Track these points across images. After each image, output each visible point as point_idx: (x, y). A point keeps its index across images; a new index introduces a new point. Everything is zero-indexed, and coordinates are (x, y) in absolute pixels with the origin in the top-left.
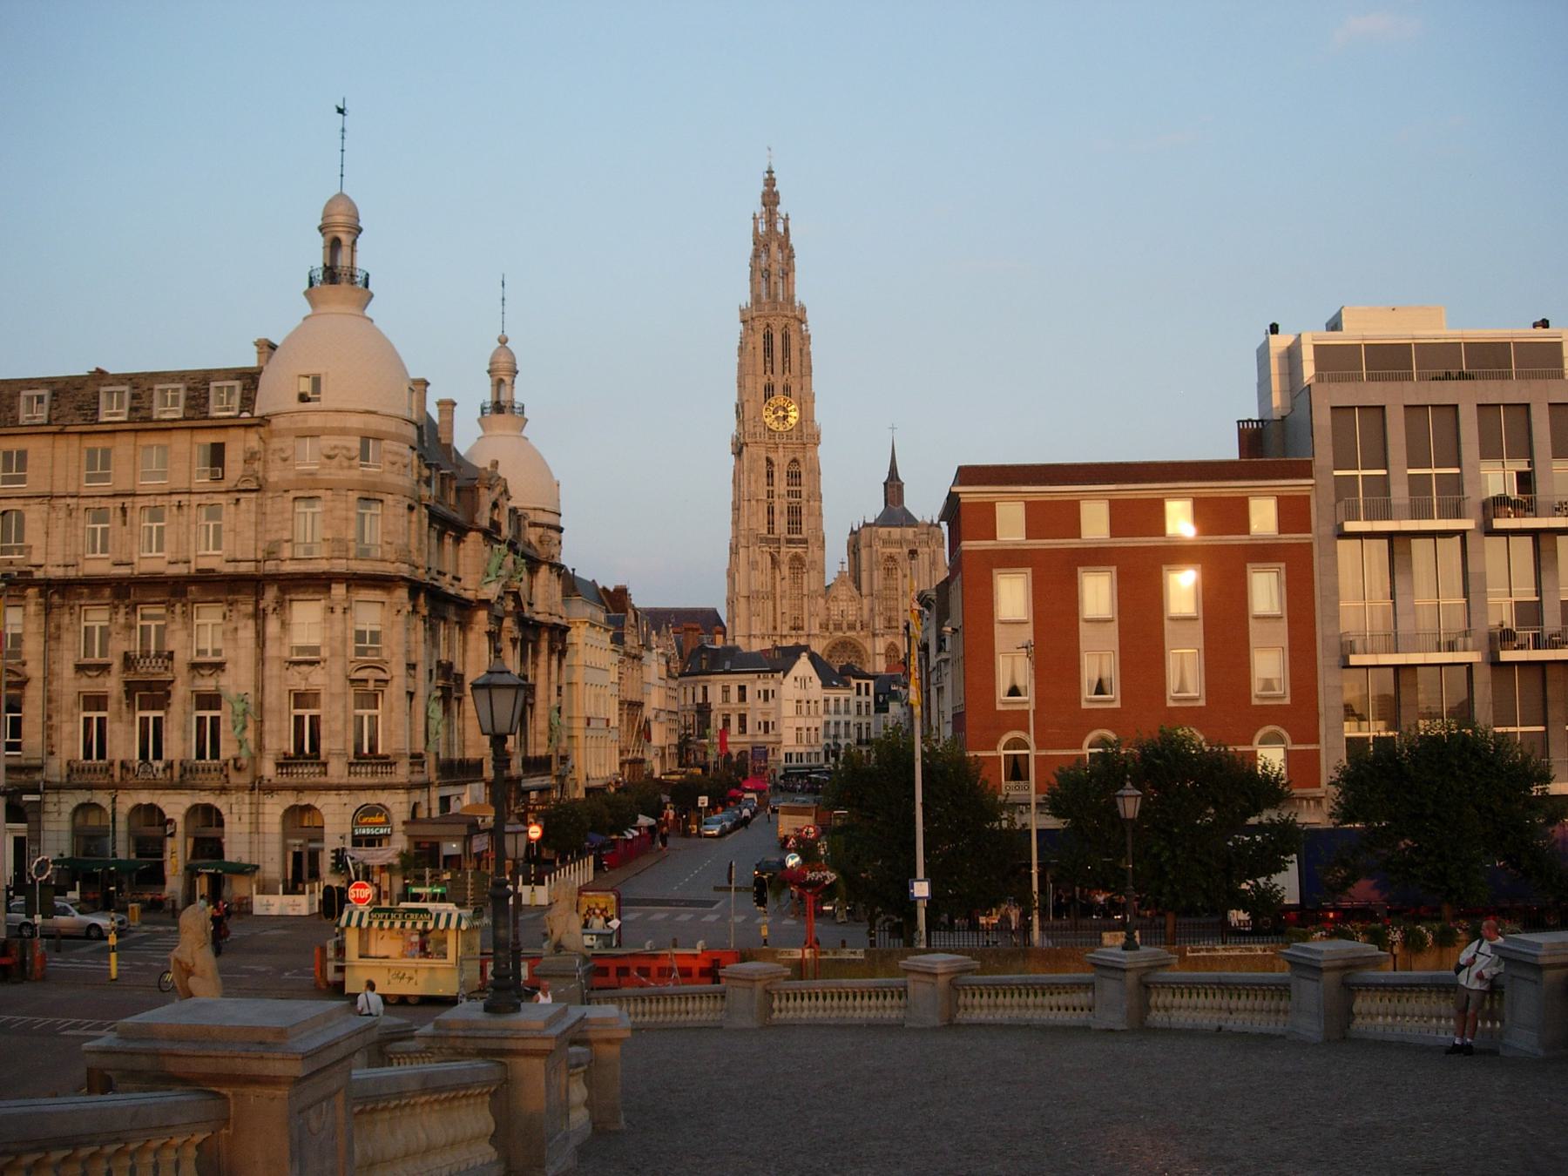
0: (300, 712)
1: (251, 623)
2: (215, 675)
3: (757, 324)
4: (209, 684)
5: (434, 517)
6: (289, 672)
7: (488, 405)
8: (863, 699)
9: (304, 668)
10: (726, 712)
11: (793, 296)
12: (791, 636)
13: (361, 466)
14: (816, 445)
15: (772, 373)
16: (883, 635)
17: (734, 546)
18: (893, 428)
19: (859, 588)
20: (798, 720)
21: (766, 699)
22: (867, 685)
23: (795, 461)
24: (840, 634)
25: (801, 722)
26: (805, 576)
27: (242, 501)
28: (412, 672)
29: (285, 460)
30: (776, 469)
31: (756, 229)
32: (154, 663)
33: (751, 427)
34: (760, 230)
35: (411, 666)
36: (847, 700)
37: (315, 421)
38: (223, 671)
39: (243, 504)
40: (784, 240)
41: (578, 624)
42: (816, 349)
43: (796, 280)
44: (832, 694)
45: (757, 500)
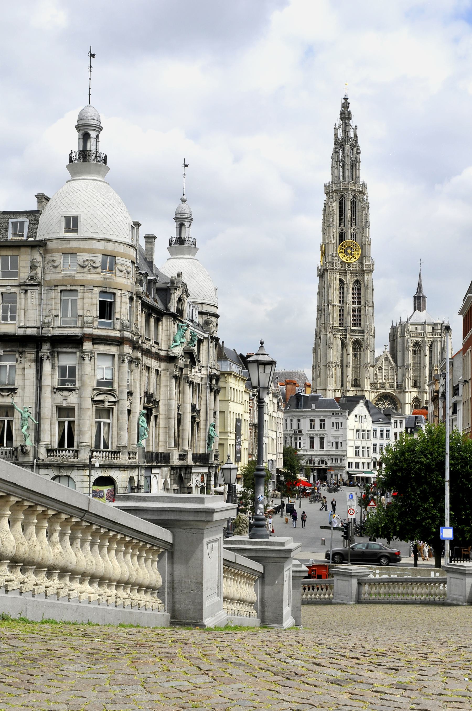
0: (62, 419)
1: (33, 365)
2: (11, 395)
3: (335, 195)
4: (7, 401)
5: (145, 305)
6: (56, 395)
7: (174, 239)
9: (65, 393)
10: (312, 436)
11: (359, 178)
13: (102, 272)
14: (371, 271)
15: (344, 226)
16: (410, 392)
17: (318, 334)
19: (396, 362)
20: (356, 442)
22: (401, 422)
23: (357, 281)
24: (384, 391)
25: (358, 443)
26: (362, 353)
27: (29, 291)
28: (130, 397)
29: (55, 267)
30: (345, 286)
31: (336, 135)
33: (330, 260)
34: (339, 136)
35: (130, 394)
36: (388, 431)
37: (74, 245)
38: (16, 393)
39: (29, 293)
41: (226, 375)
42: (371, 211)
43: (361, 168)
45: (333, 305)
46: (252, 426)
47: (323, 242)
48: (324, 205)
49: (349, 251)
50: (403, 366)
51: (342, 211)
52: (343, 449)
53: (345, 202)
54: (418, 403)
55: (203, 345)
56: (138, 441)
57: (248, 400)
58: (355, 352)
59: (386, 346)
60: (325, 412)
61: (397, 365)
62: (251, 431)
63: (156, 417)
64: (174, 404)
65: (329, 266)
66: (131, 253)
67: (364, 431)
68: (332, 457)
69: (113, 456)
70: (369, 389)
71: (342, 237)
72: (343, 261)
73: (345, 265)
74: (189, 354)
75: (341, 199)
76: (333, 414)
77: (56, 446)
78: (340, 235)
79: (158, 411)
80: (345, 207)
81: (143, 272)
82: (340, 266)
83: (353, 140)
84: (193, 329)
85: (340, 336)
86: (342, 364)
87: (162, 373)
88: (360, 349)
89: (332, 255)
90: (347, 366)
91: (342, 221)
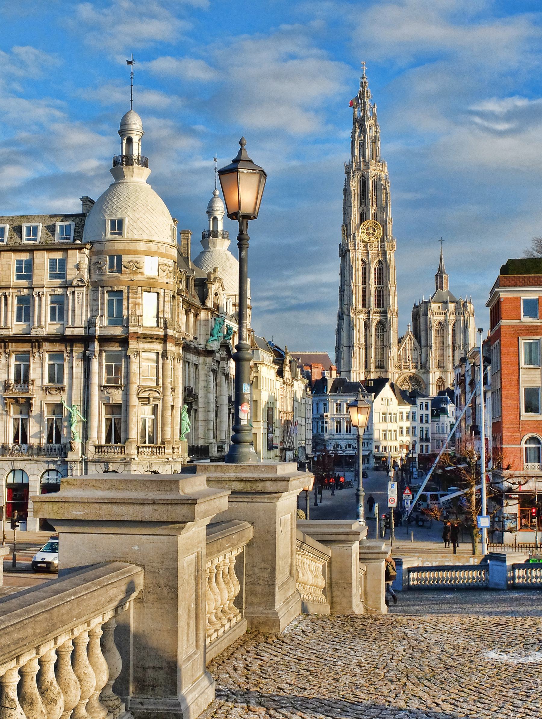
8: (424, 412)
12: (376, 372)
15: (365, 206)
19: (419, 342)
26: (385, 334)
28: (173, 393)
32: (23, 387)
35: (173, 390)
40: (373, 121)
47: (344, 222)
49: (371, 231)
50: (427, 346)
53: (365, 181)
61: (420, 346)
63: (196, 410)
64: (212, 397)
66: (173, 254)
69: (158, 451)
70: (393, 369)
73: (367, 245)
77: (103, 443)
79: (197, 404)
86: (366, 345)
87: (201, 368)
88: (383, 329)
89: (354, 236)
90: (371, 347)
91: (363, 201)
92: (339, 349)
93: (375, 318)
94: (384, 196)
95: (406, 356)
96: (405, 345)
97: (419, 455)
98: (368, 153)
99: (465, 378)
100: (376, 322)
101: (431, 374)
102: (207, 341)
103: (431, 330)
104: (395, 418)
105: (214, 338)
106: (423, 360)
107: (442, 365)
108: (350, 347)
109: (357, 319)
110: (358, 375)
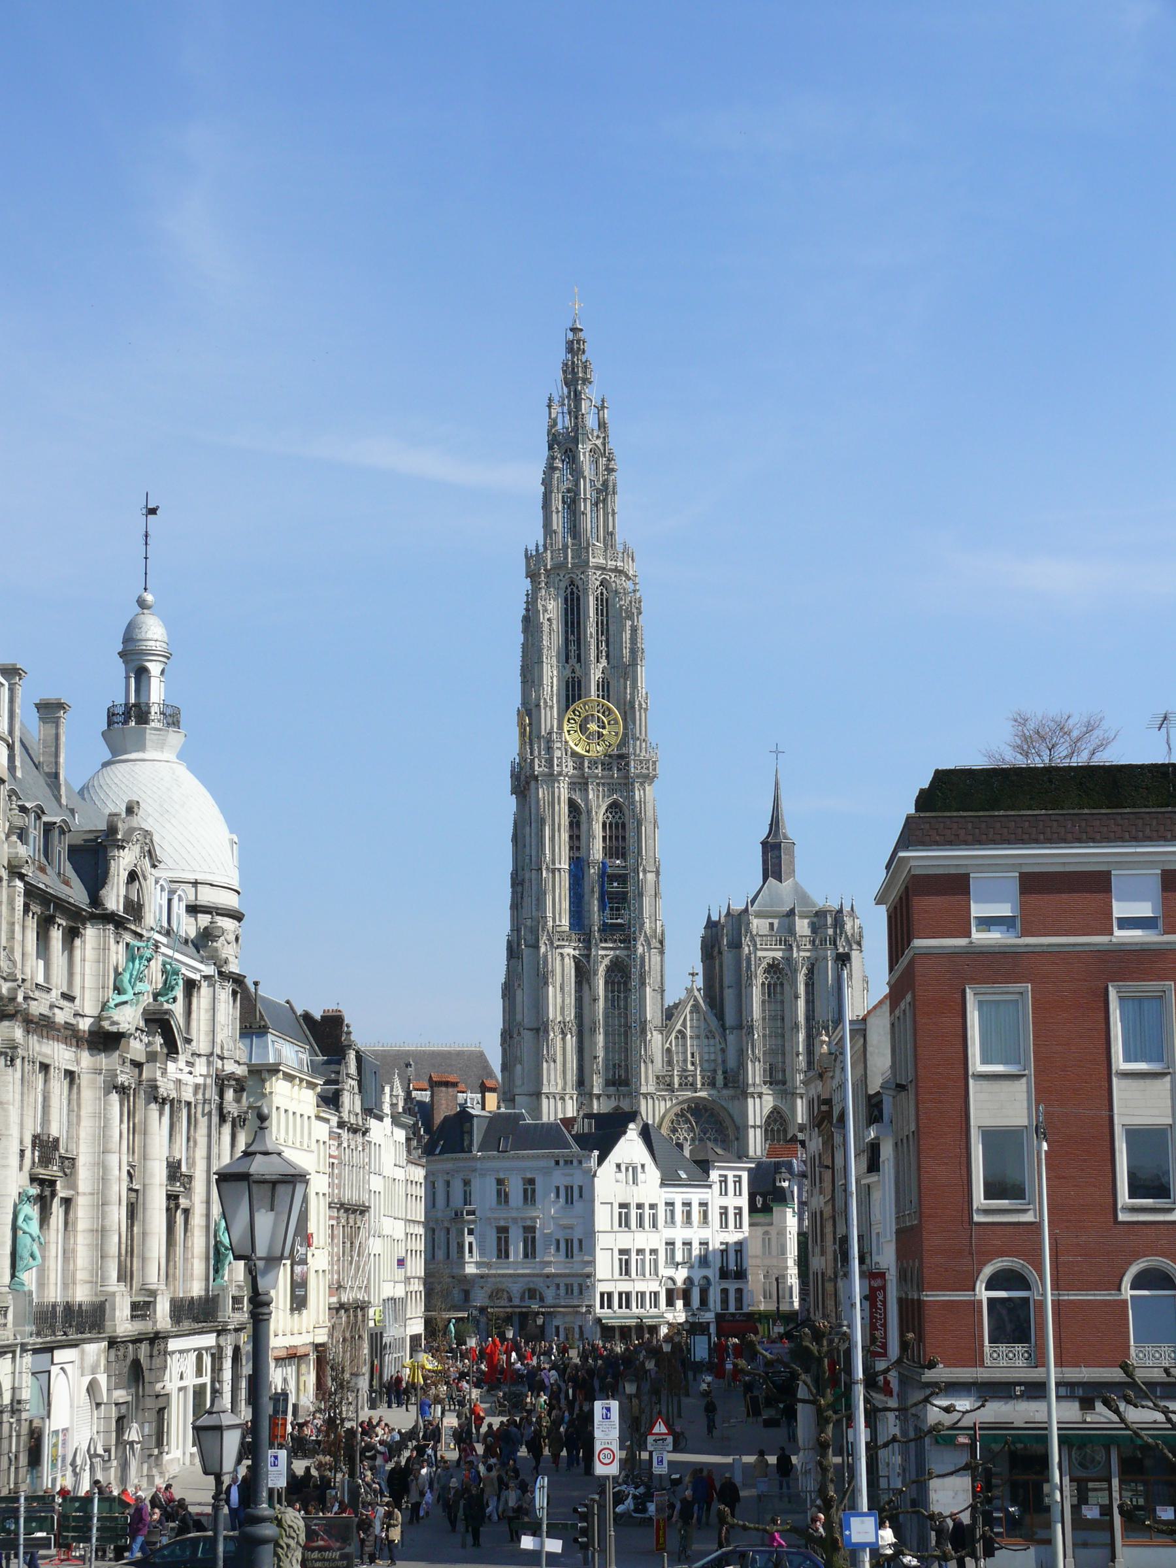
5: (32, 893)
8: (731, 1202)
10: (502, 1223)
12: (609, 1097)
15: (579, 661)
17: (515, 946)
18: (777, 752)
19: (720, 1016)
21: (569, 1201)
22: (738, 1180)
24: (689, 1094)
25: (625, 1240)
30: (584, 817)
36: (703, 1204)
40: (599, 442)
44: (678, 1195)
45: (553, 871)
46: (338, 1210)
47: (524, 704)
48: (525, 606)
49: (593, 727)
50: (740, 1027)
51: (572, 619)
52: (587, 1258)
53: (578, 599)
54: (781, 1125)
55: (199, 997)
56: (13, 1276)
57: (327, 1139)
58: (613, 992)
59: (692, 974)
60: (538, 1157)
62: (334, 1222)
63: (67, 1202)
64: (117, 1164)
65: (540, 766)
67: (640, 1206)
68: (557, 1280)
70: (651, 1089)
71: (573, 690)
72: (578, 753)
73: (582, 763)
74: (158, 1022)
75: (569, 590)
76: (557, 1163)
78: (567, 687)
79: (73, 1186)
80: (578, 609)
81: (28, 805)
82: (569, 768)
83: (598, 437)
84: (169, 952)
85: (572, 952)
87: (85, 1080)
88: (626, 984)
89: (549, 741)
90: (593, 1031)
91: (573, 648)
92: (511, 1037)
93: (604, 955)
94: (627, 635)
95: (685, 1052)
96: (684, 1025)
97: (718, 1316)
98: (587, 523)
99: (831, 1107)
100: (606, 961)
101: (750, 1101)
102: (104, 1006)
103: (751, 985)
104: (655, 1217)
105: (123, 998)
106: (732, 1063)
107: (780, 1076)
108: (540, 1029)
109: (559, 958)
110: (559, 1103)
